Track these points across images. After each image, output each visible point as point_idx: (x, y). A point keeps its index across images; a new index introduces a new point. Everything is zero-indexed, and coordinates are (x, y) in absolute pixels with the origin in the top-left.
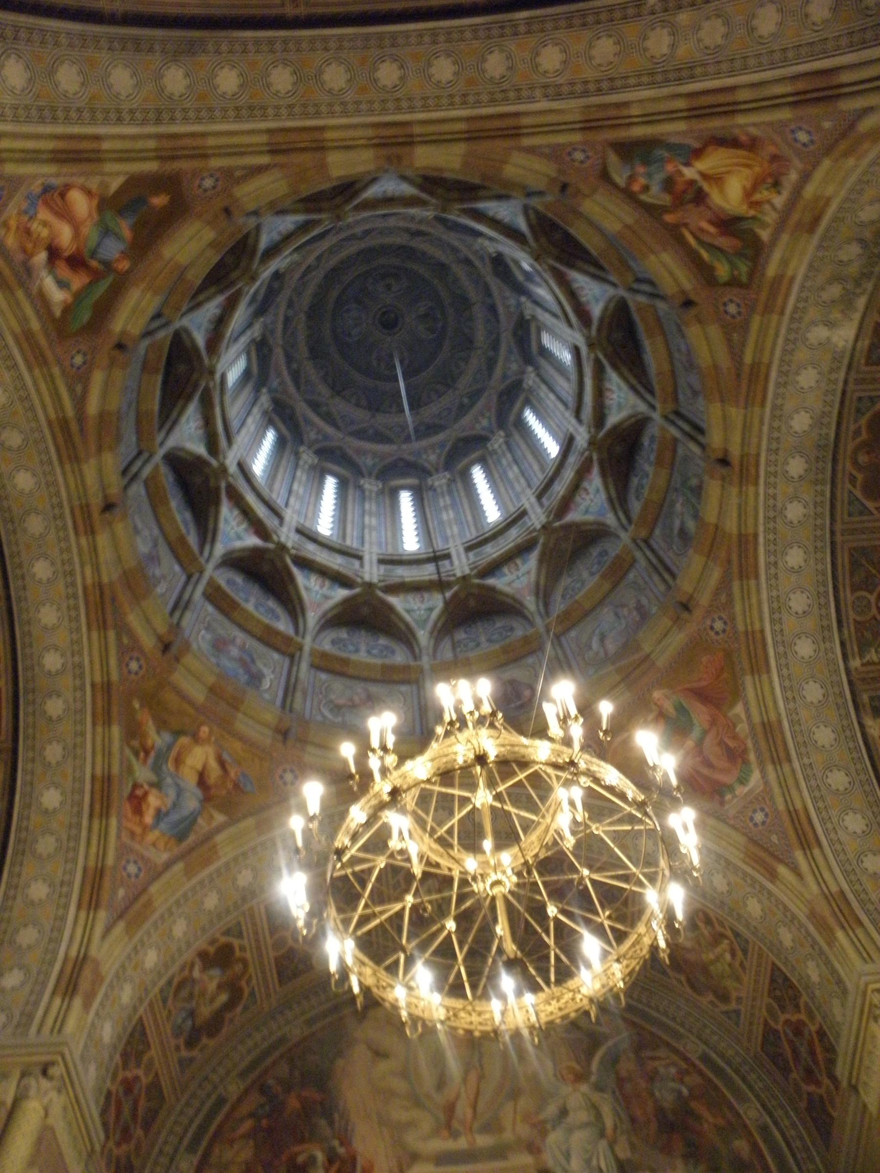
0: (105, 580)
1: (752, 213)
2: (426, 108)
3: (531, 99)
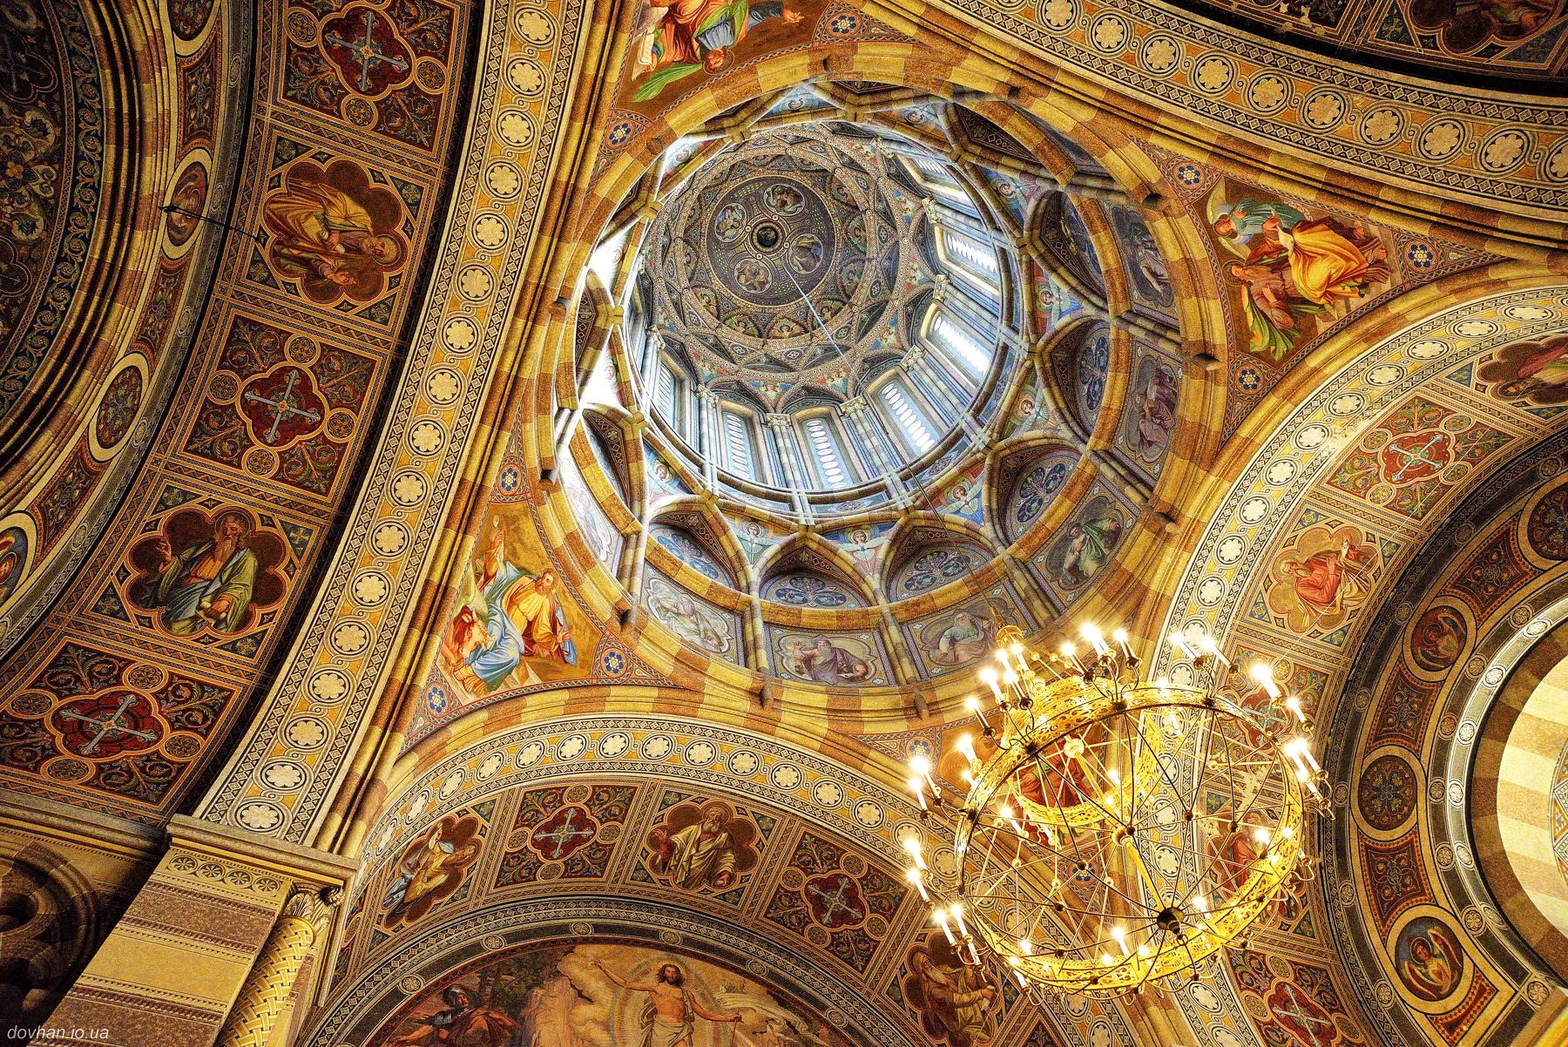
0: (525, 374)
1: (1322, 301)
2: (1076, 61)
3: (1177, 103)
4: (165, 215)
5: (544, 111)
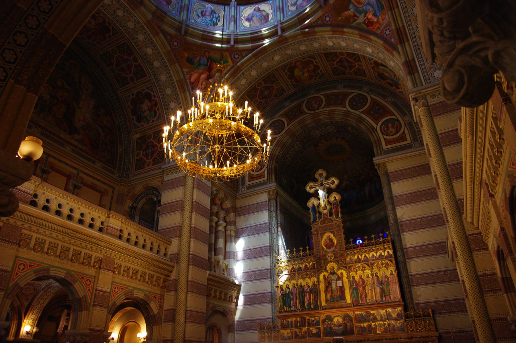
4: (316, 111)
5: (246, 74)
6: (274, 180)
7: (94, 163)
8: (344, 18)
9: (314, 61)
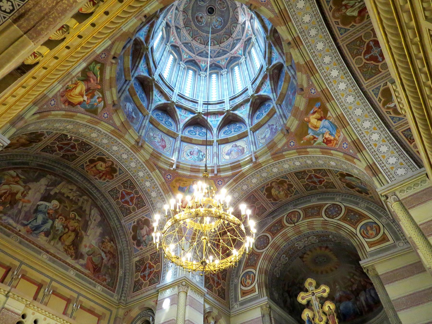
1: (78, 81)
2: (124, 147)
3: (105, 133)
6: (265, 294)
7: (95, 287)
8: (305, 141)
9: (286, 180)
